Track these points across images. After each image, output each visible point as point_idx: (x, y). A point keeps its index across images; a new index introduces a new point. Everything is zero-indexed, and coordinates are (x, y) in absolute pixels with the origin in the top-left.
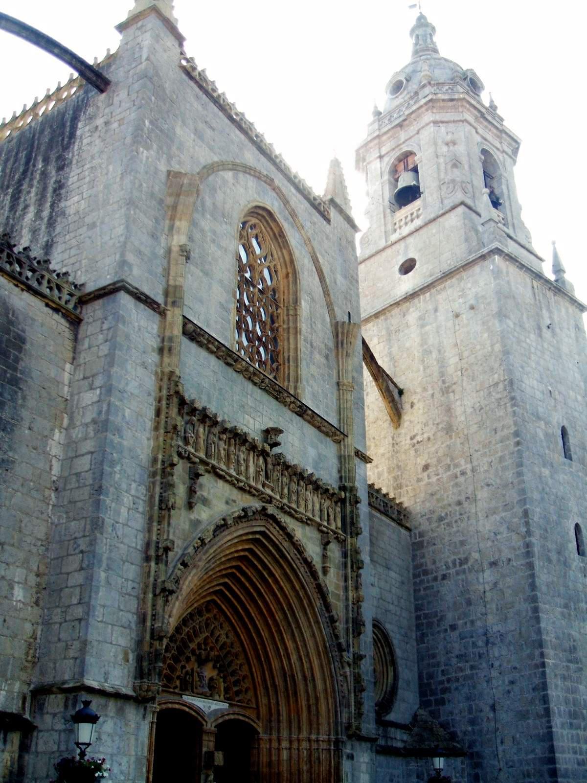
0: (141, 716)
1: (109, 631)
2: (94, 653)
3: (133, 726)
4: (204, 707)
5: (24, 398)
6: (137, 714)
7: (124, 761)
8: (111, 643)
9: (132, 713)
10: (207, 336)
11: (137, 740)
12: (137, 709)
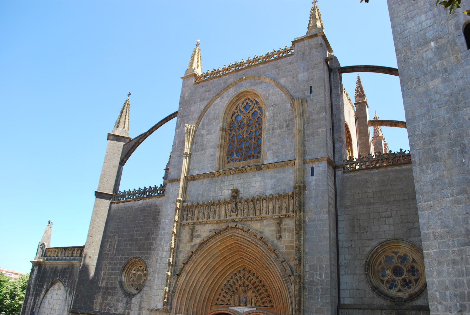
4: (240, 310)
5: (159, 228)
10: (196, 176)
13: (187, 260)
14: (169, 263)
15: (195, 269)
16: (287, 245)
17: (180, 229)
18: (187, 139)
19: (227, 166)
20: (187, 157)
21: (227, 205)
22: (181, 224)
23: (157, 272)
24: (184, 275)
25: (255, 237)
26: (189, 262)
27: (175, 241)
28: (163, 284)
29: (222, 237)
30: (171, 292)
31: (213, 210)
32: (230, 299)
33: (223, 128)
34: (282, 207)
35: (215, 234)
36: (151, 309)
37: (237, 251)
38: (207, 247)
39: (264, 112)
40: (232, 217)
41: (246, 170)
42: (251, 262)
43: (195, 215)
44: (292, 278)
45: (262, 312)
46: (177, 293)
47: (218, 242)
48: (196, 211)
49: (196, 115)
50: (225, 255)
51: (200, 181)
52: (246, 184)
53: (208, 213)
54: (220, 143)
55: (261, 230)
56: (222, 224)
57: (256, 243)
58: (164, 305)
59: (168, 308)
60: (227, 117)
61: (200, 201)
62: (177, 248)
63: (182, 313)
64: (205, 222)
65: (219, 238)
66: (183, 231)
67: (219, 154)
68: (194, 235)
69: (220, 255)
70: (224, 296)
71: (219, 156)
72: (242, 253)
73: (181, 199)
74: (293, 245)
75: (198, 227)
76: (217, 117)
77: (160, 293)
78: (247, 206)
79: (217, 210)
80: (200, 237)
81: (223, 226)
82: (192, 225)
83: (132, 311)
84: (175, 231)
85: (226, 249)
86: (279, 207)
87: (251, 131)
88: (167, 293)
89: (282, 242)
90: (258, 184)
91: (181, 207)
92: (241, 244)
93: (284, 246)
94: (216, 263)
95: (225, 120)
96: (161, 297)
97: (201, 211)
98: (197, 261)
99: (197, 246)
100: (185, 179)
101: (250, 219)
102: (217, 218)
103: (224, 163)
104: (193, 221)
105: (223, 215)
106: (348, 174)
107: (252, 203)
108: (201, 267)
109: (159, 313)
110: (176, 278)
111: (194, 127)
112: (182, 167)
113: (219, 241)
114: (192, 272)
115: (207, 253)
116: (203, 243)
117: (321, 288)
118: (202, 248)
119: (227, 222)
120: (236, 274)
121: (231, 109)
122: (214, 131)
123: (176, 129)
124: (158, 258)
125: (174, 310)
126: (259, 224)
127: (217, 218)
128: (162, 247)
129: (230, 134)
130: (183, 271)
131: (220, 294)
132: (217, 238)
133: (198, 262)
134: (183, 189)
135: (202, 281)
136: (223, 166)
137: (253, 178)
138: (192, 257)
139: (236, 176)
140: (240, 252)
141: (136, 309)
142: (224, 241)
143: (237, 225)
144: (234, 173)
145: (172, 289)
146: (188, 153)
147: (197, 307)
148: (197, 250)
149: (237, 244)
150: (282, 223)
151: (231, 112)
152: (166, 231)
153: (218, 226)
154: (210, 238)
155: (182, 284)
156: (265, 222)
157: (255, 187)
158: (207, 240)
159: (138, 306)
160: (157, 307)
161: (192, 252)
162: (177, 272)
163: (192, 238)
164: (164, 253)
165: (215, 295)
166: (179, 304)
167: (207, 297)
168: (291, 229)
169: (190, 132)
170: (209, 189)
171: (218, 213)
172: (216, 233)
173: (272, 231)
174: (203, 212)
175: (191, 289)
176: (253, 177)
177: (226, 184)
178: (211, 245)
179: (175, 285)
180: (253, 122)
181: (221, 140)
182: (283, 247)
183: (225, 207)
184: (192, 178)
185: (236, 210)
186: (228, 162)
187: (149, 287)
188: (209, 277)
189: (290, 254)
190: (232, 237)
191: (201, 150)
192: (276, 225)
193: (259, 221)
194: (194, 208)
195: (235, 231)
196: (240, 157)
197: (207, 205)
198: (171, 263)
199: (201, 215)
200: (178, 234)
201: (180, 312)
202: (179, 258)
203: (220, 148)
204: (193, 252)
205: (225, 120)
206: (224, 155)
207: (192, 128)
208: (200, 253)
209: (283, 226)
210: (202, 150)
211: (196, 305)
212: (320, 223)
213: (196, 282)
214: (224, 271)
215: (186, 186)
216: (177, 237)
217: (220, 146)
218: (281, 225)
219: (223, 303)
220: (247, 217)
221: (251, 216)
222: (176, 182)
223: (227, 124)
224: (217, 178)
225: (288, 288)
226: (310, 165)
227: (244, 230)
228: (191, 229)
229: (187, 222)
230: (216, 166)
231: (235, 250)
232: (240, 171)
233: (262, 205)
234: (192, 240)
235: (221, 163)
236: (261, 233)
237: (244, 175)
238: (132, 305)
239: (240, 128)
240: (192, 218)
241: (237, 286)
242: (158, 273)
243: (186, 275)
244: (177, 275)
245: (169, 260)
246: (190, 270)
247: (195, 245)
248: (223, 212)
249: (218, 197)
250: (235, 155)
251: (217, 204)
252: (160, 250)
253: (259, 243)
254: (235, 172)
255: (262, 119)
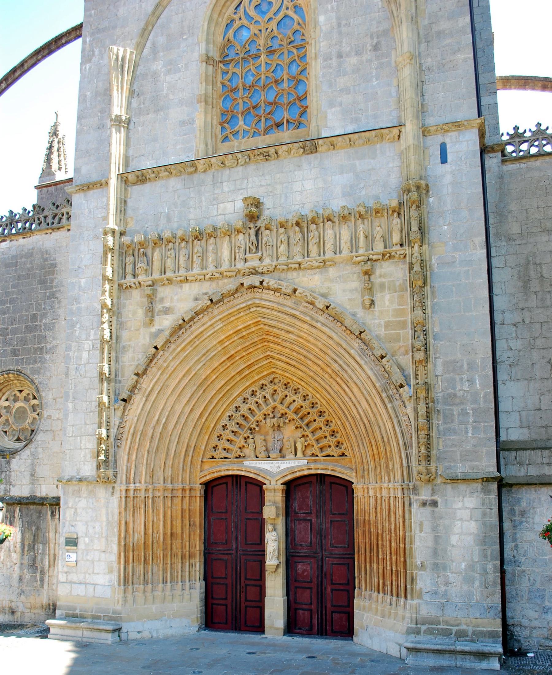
0: (110, 494)
1: (79, 441)
2: (68, 458)
3: (103, 501)
4: (271, 467)
6: (106, 492)
7: (97, 525)
8: (81, 449)
9: (102, 492)
11: (107, 510)
12: (106, 489)
13: (144, 367)
14: (101, 374)
15: (163, 385)
16: (389, 321)
17: (119, 298)
18: (118, 82)
19: (224, 148)
20: (120, 126)
21: (233, 236)
22: (120, 285)
23: (71, 398)
24: (138, 400)
25: (311, 307)
26: (149, 369)
27: (111, 326)
28: (88, 422)
29: (228, 310)
30: (112, 439)
31: (201, 250)
32: (244, 446)
33: (208, 58)
34: (372, 235)
35: (209, 302)
36: (66, 478)
37: (258, 342)
38: (192, 334)
39: (314, 15)
40: (250, 264)
41: (276, 153)
42: (294, 363)
43: (155, 263)
44: (406, 392)
45: (322, 467)
46: (127, 440)
47: (217, 321)
48: (155, 254)
49: (135, 28)
50: (232, 352)
51: (160, 183)
52: (279, 187)
53: (187, 256)
54: (203, 92)
55: (324, 291)
56: (226, 281)
57: (312, 318)
58: (98, 467)
59: (110, 473)
60: (215, 30)
61: (162, 231)
62: (117, 340)
63: (140, 482)
64: (182, 278)
65: (218, 312)
66: (128, 302)
67: (203, 117)
68: (156, 310)
69: (220, 351)
70: (228, 440)
71: (202, 125)
72: (271, 345)
73: (116, 228)
74: (402, 319)
75: (163, 292)
76: (189, 31)
77: (83, 442)
78: (286, 238)
79: (210, 248)
80: (173, 314)
81: (230, 285)
82: (150, 286)
83: (14, 486)
84: (109, 302)
85: (236, 338)
86: (366, 237)
87: (277, 64)
88: (102, 442)
89: (377, 314)
90: (309, 185)
91: (117, 247)
92: (270, 326)
93: (382, 322)
94: (212, 370)
95: (211, 37)
96: (87, 451)
97: (169, 253)
98: (167, 367)
99: (167, 333)
100: (122, 180)
101: (297, 266)
102: (211, 268)
103: (216, 141)
104: (150, 278)
105: (226, 260)
106: (514, 165)
107: (297, 229)
108: (178, 380)
109: (87, 485)
110: (122, 407)
111: (132, 53)
112: (109, 151)
113: (220, 319)
114: (157, 392)
115: (191, 349)
116: (180, 327)
117: (473, 409)
118: (179, 337)
119: (238, 276)
120: (253, 393)
121: (224, 11)
122: (186, 64)
123: (82, 64)
124: (71, 366)
125: (122, 477)
126: (317, 277)
127: (211, 268)
128: (77, 342)
129: (225, 73)
130: (136, 391)
131: (220, 437)
132: (216, 312)
133: (171, 369)
134: (119, 205)
135: (180, 411)
136: (213, 147)
137: (296, 173)
138: (155, 360)
139: (251, 168)
140: (266, 343)
141: (24, 481)
142: (232, 319)
143: (263, 281)
144: (247, 160)
145: (113, 432)
146: (124, 118)
147: (172, 468)
148: (168, 342)
149: (262, 326)
150: (374, 273)
151: (225, 20)
152: (83, 305)
153: (214, 285)
154: (197, 314)
155: (136, 418)
156: (332, 272)
157: (301, 192)
158: (192, 319)
159: (27, 474)
160: (80, 474)
161: (156, 348)
162: (124, 394)
163: (153, 316)
164: (83, 355)
165: (208, 439)
166: (134, 463)
167: (193, 445)
168: (398, 284)
169: (123, 67)
170: (184, 201)
171: (213, 255)
172: (214, 301)
173: (351, 291)
174: (173, 255)
175: (157, 430)
176: (295, 171)
177: (226, 189)
178: (201, 330)
179: (120, 423)
180: (281, 43)
181: (204, 84)
182: (379, 325)
183: (231, 242)
184: (138, 177)
185: (257, 248)
186: (225, 139)
187: (49, 432)
188: (196, 402)
189: (397, 339)
190: (250, 309)
191: (155, 111)
192: (359, 277)
193: (318, 270)
194: (150, 247)
195: (258, 295)
196: (254, 126)
197: (184, 240)
198: (107, 375)
199: (169, 263)
200: (115, 308)
201: (137, 480)
202: (123, 362)
203: (203, 104)
204: (158, 347)
205: (211, 37)
206: (215, 122)
207: (128, 55)
208: (174, 350)
209: (376, 279)
210: (158, 110)
211: (170, 463)
212: (466, 268)
213: (167, 414)
214: (228, 388)
215: (125, 197)
216: (114, 315)
217: (203, 99)
218: (372, 277)
219: (228, 455)
220: (289, 261)
221: (298, 259)
222: (95, 191)
223: (215, 48)
224: (202, 176)
225: (396, 413)
226: (439, 139)
227: (283, 290)
228: (149, 296)
229: (136, 280)
230: (196, 146)
231: (256, 340)
232: (262, 156)
233: (322, 232)
234: (152, 321)
235: (209, 142)
236: (324, 296)
237: (272, 165)
238: (13, 474)
239: (250, 56)
240: (146, 270)
241: (259, 416)
242: (75, 398)
243: (144, 399)
244: (124, 400)
245: (101, 368)
246: (152, 389)
247: (160, 331)
248: (226, 253)
249: (208, 218)
250: (241, 123)
251: (210, 236)
252: (73, 349)
253: (321, 318)
254: (250, 159)
255: (303, 35)
